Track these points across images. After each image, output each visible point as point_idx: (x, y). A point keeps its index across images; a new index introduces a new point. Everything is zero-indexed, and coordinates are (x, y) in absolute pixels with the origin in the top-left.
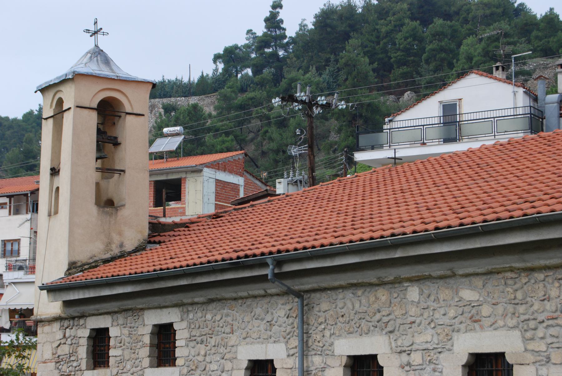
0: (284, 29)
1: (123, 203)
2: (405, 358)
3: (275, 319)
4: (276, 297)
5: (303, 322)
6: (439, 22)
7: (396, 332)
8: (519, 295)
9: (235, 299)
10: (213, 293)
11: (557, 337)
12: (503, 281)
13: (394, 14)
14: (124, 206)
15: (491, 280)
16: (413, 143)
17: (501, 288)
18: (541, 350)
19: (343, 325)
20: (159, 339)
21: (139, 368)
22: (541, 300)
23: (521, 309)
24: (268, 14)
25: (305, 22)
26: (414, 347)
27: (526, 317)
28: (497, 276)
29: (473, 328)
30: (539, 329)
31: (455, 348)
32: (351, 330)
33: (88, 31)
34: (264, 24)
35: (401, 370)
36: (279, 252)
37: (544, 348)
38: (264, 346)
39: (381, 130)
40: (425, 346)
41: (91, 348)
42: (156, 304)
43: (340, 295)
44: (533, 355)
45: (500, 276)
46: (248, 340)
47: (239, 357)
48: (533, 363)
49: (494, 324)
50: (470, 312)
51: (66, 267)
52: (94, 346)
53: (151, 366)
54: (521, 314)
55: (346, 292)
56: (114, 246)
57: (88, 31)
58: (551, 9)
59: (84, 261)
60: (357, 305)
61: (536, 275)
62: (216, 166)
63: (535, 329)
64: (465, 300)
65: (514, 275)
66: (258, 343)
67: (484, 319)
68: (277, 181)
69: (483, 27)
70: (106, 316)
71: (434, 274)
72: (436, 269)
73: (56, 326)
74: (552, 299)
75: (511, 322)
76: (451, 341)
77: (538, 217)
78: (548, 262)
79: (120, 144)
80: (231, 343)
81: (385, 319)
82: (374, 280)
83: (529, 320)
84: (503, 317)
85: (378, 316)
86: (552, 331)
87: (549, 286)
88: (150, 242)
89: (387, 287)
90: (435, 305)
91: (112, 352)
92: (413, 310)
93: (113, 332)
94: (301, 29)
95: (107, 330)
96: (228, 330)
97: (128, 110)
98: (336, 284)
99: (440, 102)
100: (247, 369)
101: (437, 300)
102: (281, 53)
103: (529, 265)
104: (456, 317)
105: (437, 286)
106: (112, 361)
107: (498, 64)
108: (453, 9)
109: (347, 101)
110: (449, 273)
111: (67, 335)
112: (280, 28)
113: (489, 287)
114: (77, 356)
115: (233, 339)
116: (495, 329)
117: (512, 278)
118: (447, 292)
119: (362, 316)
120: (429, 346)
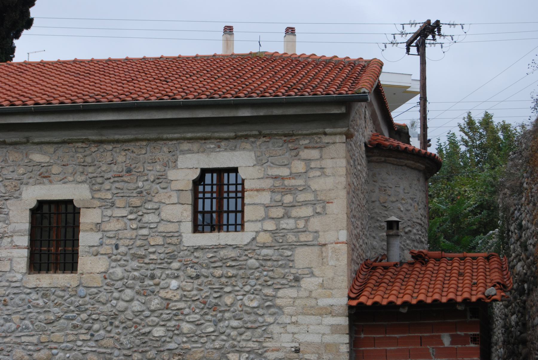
8: (89, 159)
11: (122, 189)
12: (73, 149)
15: (62, 148)
17: (71, 154)
18: (107, 198)
22: (109, 164)
23: (91, 169)
27: (95, 175)
28: (67, 145)
30: (105, 184)
31: (24, 196)
37: (109, 196)
44: (99, 201)
45: (71, 145)
48: (99, 207)
49: (63, 179)
50: (39, 170)
54: (90, 173)
61: (105, 146)
64: (34, 161)
65: (84, 145)
67: (53, 176)
71: (8, 140)
74: (118, 163)
75: (79, 178)
76: (19, 191)
77: (136, 103)
78: (121, 137)
83: (97, 177)
84: (72, 175)
86: (117, 185)
87: (115, 155)
103: (104, 138)
105: (5, 150)
110: (24, 140)
113: (60, 152)
116: (65, 183)
117: (82, 147)
118: (16, 155)
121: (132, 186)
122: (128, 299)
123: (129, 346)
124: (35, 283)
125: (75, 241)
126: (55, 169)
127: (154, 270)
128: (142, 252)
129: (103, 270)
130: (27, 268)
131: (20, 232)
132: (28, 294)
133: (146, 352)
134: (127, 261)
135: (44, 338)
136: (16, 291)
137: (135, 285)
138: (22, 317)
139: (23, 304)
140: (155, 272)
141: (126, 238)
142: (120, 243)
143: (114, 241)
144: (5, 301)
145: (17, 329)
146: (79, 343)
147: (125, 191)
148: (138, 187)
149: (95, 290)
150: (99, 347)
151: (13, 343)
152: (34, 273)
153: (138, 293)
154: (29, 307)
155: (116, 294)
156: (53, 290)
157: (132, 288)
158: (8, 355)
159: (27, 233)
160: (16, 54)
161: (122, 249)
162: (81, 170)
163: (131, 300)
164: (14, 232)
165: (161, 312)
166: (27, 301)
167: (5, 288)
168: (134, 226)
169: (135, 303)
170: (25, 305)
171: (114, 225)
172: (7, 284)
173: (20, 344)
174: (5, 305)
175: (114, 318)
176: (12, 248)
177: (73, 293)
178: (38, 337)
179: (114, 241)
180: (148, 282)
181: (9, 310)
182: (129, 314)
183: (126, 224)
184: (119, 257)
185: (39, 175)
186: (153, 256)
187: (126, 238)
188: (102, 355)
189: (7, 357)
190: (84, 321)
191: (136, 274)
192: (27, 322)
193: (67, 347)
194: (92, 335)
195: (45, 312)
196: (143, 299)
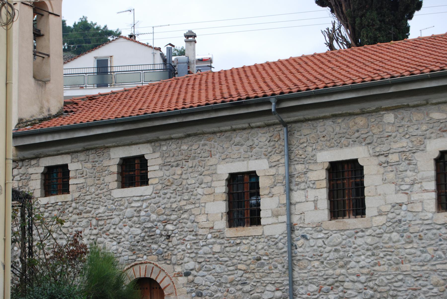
1: (48, 79)
2: (382, 159)
3: (256, 143)
4: (256, 129)
7: (373, 143)
9: (214, 133)
14: (49, 81)
16: (73, 86)
19: (324, 143)
20: (122, 168)
21: (105, 190)
26: (391, 151)
29: (442, 135)
31: (428, 148)
32: (332, 145)
35: (379, 167)
38: (245, 162)
41: (43, 182)
42: (128, 142)
43: (320, 124)
47: (219, 172)
50: (439, 126)
52: (45, 180)
53: (118, 188)
55: (325, 121)
56: (44, 110)
64: (434, 119)
66: (239, 161)
70: (65, 156)
71: (411, 104)
76: (423, 145)
79: (43, 35)
80: (211, 163)
81: (365, 136)
85: (357, 135)
89: (365, 115)
90: (409, 124)
91: (71, 182)
92: (390, 128)
93: (71, 167)
95: (66, 166)
96: (206, 155)
97: (50, 11)
99: (95, 58)
101: (410, 121)
104: (427, 130)
105: (409, 112)
106: (71, 188)
110: (424, 102)
114: (29, 188)
115: (213, 161)
118: (419, 115)
120: (404, 149)
124: (444, 220)
131: (428, 179)
132: (439, 229)
136: (428, 227)
138: (435, 248)
139: (435, 238)
144: (420, 236)
145: (432, 258)
151: (429, 271)
152: (442, 212)
158: (427, 280)
159: (434, 179)
160: (410, 32)
164: (422, 179)
166: (438, 235)
167: (419, 226)
170: (437, 238)
172: (421, 222)
173: (435, 271)
174: (421, 239)
176: (422, 192)
181: (423, 243)
185: (439, 130)
189: (425, 282)
192: (440, 253)
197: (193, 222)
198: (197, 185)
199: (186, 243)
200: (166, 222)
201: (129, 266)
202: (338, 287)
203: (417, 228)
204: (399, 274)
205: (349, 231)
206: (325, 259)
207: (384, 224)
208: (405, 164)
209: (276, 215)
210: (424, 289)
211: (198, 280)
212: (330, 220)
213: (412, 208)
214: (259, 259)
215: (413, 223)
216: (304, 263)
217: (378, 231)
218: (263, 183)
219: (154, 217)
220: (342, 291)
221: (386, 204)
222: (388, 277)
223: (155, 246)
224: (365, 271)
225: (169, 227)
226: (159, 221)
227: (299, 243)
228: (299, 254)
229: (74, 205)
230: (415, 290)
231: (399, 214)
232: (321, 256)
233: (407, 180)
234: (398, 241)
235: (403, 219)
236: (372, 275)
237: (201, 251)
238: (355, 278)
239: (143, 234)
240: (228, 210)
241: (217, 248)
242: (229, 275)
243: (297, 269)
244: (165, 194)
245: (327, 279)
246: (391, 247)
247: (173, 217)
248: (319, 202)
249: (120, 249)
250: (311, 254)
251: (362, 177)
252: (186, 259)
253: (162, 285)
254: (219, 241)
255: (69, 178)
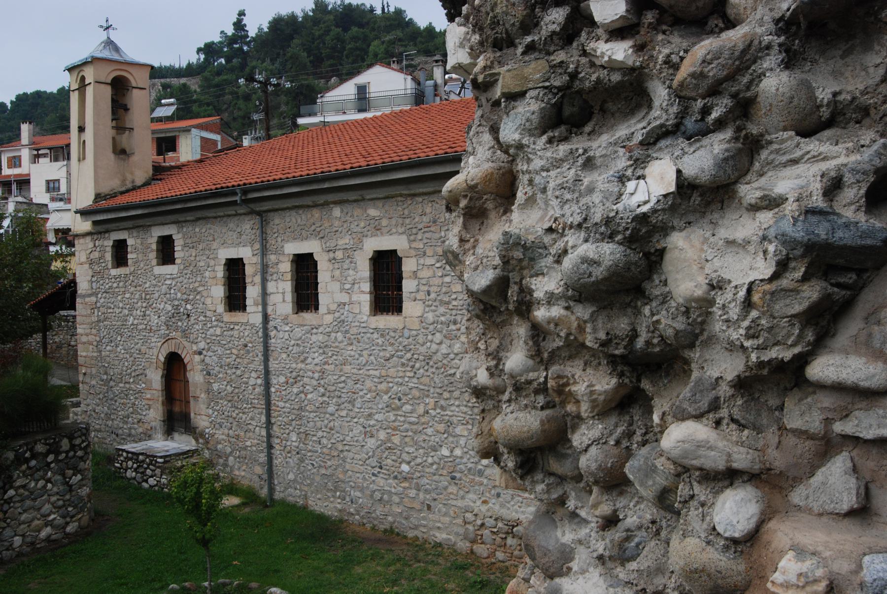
0: (247, 31)
2: (331, 255)
4: (243, 216)
5: (262, 232)
6: (354, 29)
8: (406, 212)
9: (215, 218)
10: (199, 214)
13: (324, 23)
14: (133, 153)
17: (394, 207)
23: (407, 221)
24: (235, 20)
25: (262, 27)
26: (338, 247)
27: (411, 226)
33: (101, 27)
34: (232, 27)
36: (245, 184)
39: (315, 103)
40: (345, 247)
41: (114, 254)
42: (159, 222)
45: (394, 199)
46: (225, 245)
51: (93, 197)
53: (158, 264)
56: (127, 182)
57: (101, 27)
58: (430, 23)
59: (107, 193)
60: (299, 220)
62: (200, 127)
63: (416, 234)
65: (402, 199)
68: (244, 137)
69: (385, 34)
72: (352, 196)
73: (88, 239)
75: (401, 230)
78: (425, 190)
80: (213, 248)
81: (318, 229)
82: (310, 203)
85: (313, 227)
86: (427, 235)
87: (425, 206)
88: (154, 179)
90: (351, 219)
91: (129, 256)
92: (337, 223)
93: (130, 242)
94: (259, 32)
95: (125, 240)
96: (211, 239)
97: (134, 84)
98: (285, 206)
99: (356, 84)
100: (225, 265)
102: (245, 48)
103: (412, 192)
106: (130, 262)
107: (394, 59)
108: (365, 20)
109: (292, 82)
110: (360, 198)
111: (97, 245)
112: (244, 30)
113: (387, 207)
115: (215, 245)
118: (359, 210)
119: (303, 227)
120: (347, 246)
121: (437, 236)
122: (438, 342)
123: (440, 385)
125: (400, 288)
126: (384, 222)
127: (456, 315)
128: (446, 299)
129: (420, 315)
130: (371, 310)
132: (372, 333)
133: (453, 391)
134: (437, 307)
135: (384, 373)
137: (442, 329)
138: (369, 353)
140: (456, 317)
141: (435, 285)
142: (432, 289)
143: (426, 288)
146: (407, 379)
147: (433, 240)
148: (441, 237)
149: (414, 333)
150: (421, 384)
153: (445, 337)
154: (373, 345)
155: (430, 337)
156: (387, 331)
157: (441, 332)
159: (368, 280)
161: (433, 296)
162: (401, 222)
163: (440, 343)
165: (461, 355)
168: (440, 274)
169: (444, 346)
171: (425, 273)
172: (358, 324)
173: (368, 376)
175: (429, 359)
177: (401, 334)
178: (379, 371)
179: (426, 288)
180: (452, 327)
182: (439, 356)
183: (434, 271)
184: (430, 303)
186: (454, 303)
187: (435, 285)
188: (422, 391)
190: (409, 360)
191: (443, 319)
192: (372, 358)
193: (398, 382)
194: (415, 373)
195: (383, 349)
196: (448, 342)
197: (203, 304)
198: (206, 268)
199: (200, 323)
200: (187, 301)
201: (164, 340)
202: (300, 381)
203: (354, 331)
204: (342, 375)
205: (305, 328)
206: (291, 352)
207: (331, 323)
208: (348, 261)
209: (256, 304)
210: (361, 393)
211: (207, 360)
212: (297, 313)
213: (352, 309)
214: (246, 346)
215: (353, 324)
216: (275, 354)
217: (328, 330)
218: (249, 270)
219: (179, 295)
220: (303, 386)
221: (334, 303)
222: (334, 377)
223: (180, 324)
224: (318, 368)
225: (189, 307)
226: (182, 300)
227: (272, 334)
228: (272, 345)
229: (131, 278)
230: (355, 393)
231: (343, 314)
232: (288, 348)
233: (349, 279)
234: (342, 342)
235: (346, 319)
236: (323, 373)
237: (208, 333)
238: (310, 374)
239: (173, 311)
240: (227, 294)
241: (218, 331)
242: (227, 358)
243: (271, 360)
244: (186, 274)
245: (291, 372)
246: (337, 347)
247: (191, 297)
248: (286, 294)
249: (160, 323)
250: (279, 346)
251: (317, 272)
252: (199, 338)
253: (186, 361)
254: (220, 324)
255: (127, 253)
